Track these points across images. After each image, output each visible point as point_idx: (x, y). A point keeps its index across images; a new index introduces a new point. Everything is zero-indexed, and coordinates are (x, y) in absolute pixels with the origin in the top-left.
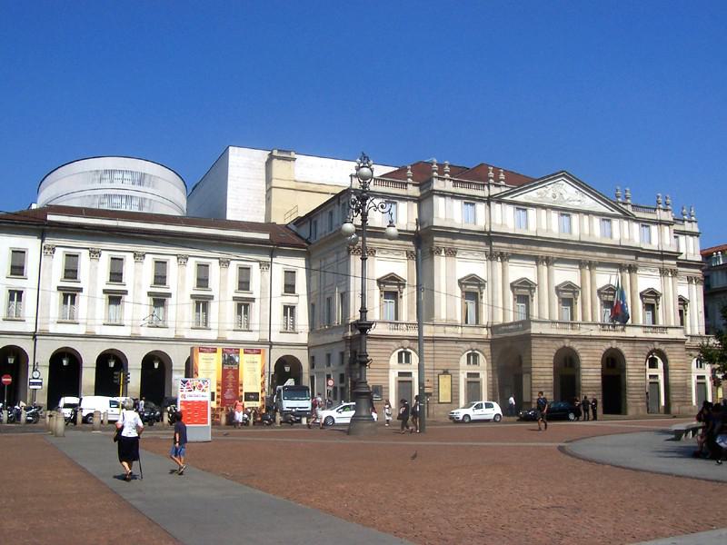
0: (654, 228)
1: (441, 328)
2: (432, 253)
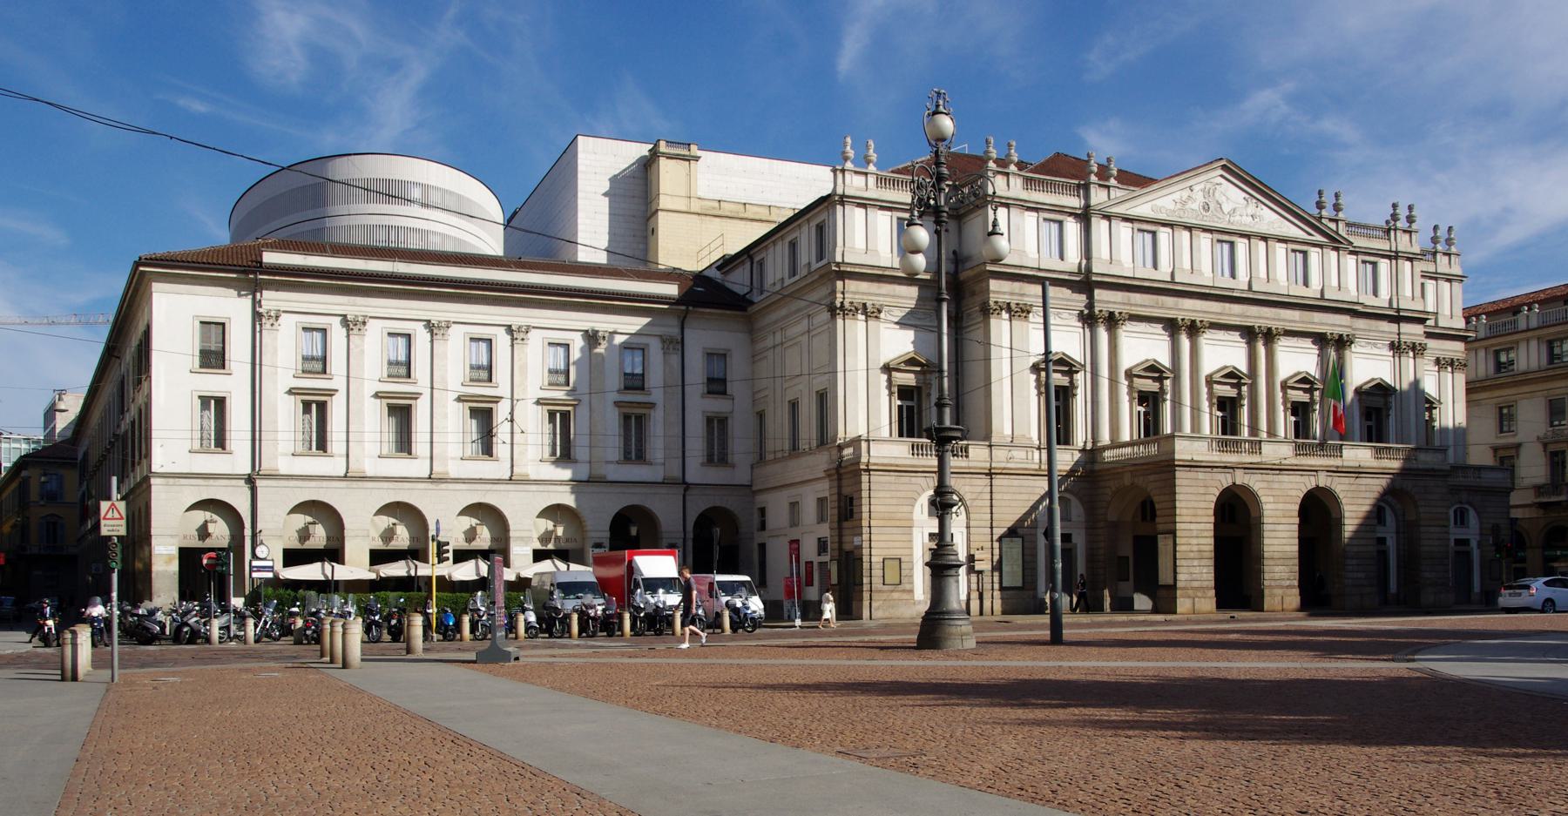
0: (1384, 265)
2: (986, 311)
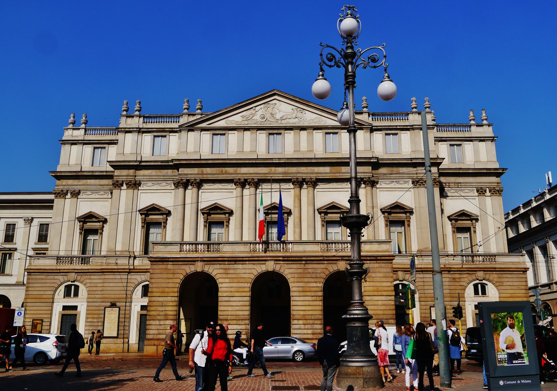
1: (112, 261)
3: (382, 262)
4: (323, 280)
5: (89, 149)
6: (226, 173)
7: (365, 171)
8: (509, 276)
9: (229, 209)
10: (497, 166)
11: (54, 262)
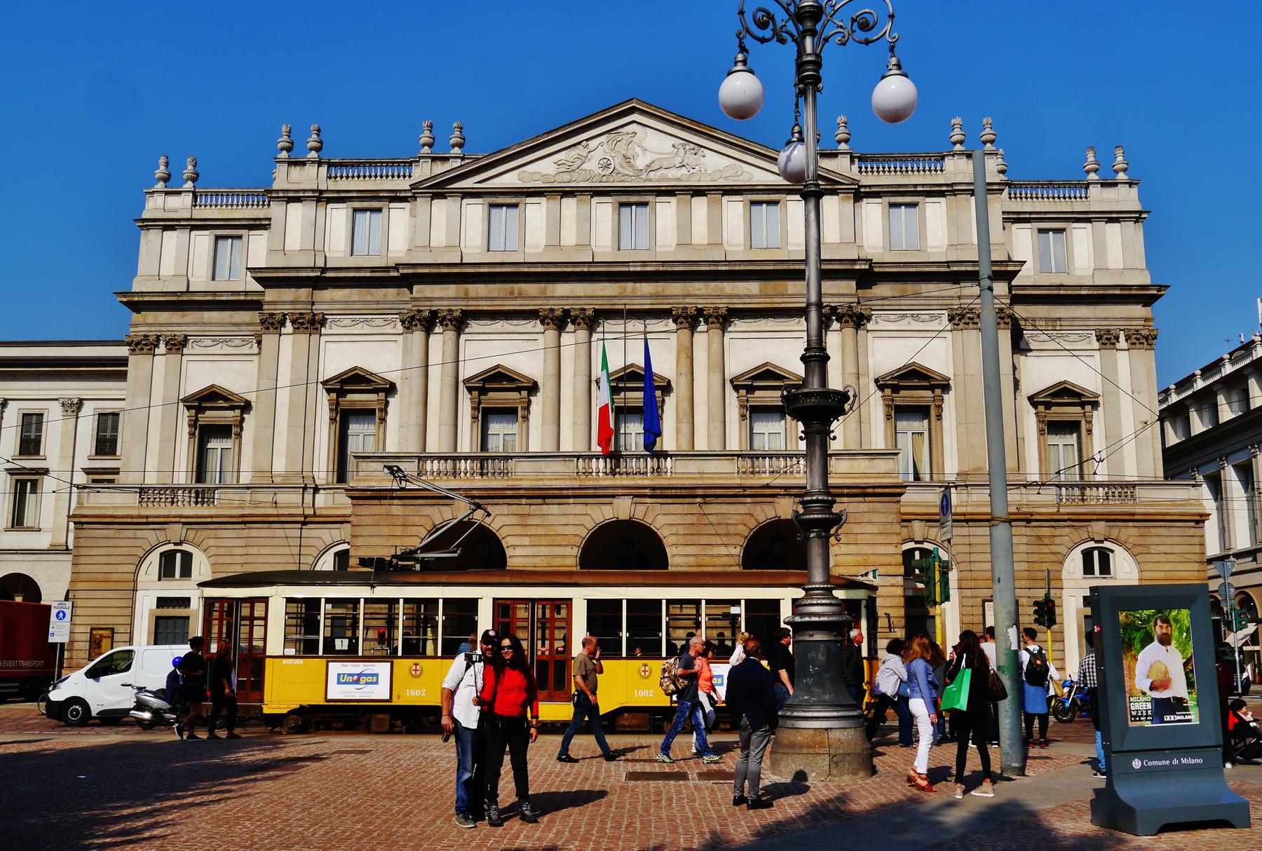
1: (265, 497)
3: (875, 499)
4: (742, 541)
5: (203, 240)
6: (521, 296)
7: (840, 292)
8: (1164, 532)
9: (529, 379)
10: (1145, 279)
11: (133, 499)
